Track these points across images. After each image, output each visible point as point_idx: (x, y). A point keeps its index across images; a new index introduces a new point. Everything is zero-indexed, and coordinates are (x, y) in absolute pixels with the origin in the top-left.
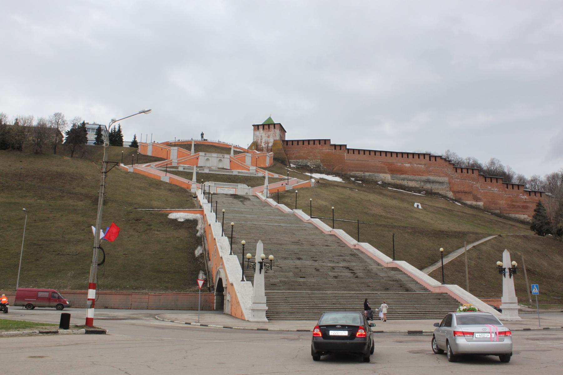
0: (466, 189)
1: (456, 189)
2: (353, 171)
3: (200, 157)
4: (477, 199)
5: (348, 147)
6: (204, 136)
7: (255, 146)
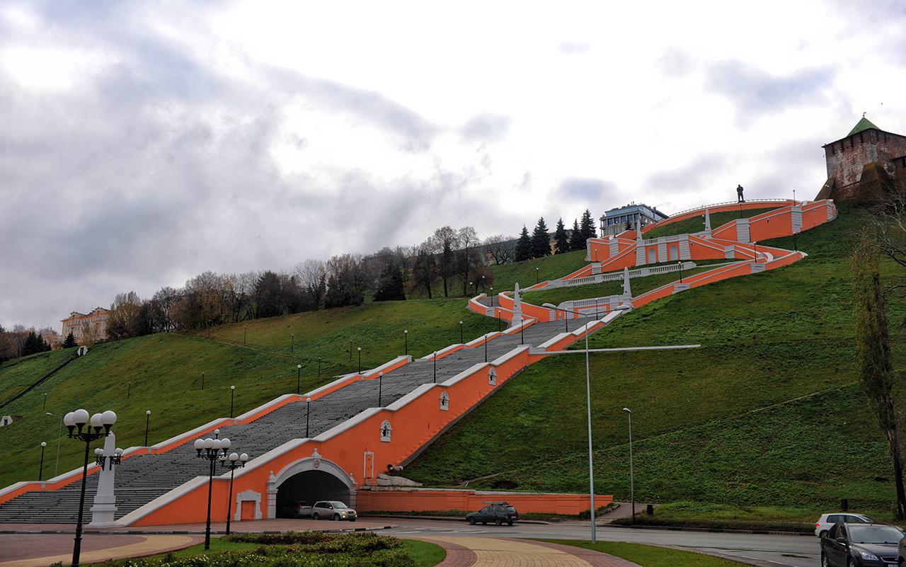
7: (832, 190)
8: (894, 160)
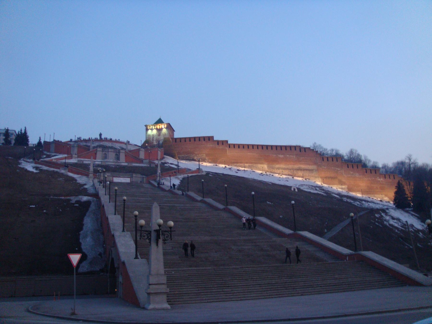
3: (98, 153)
5: (229, 143)
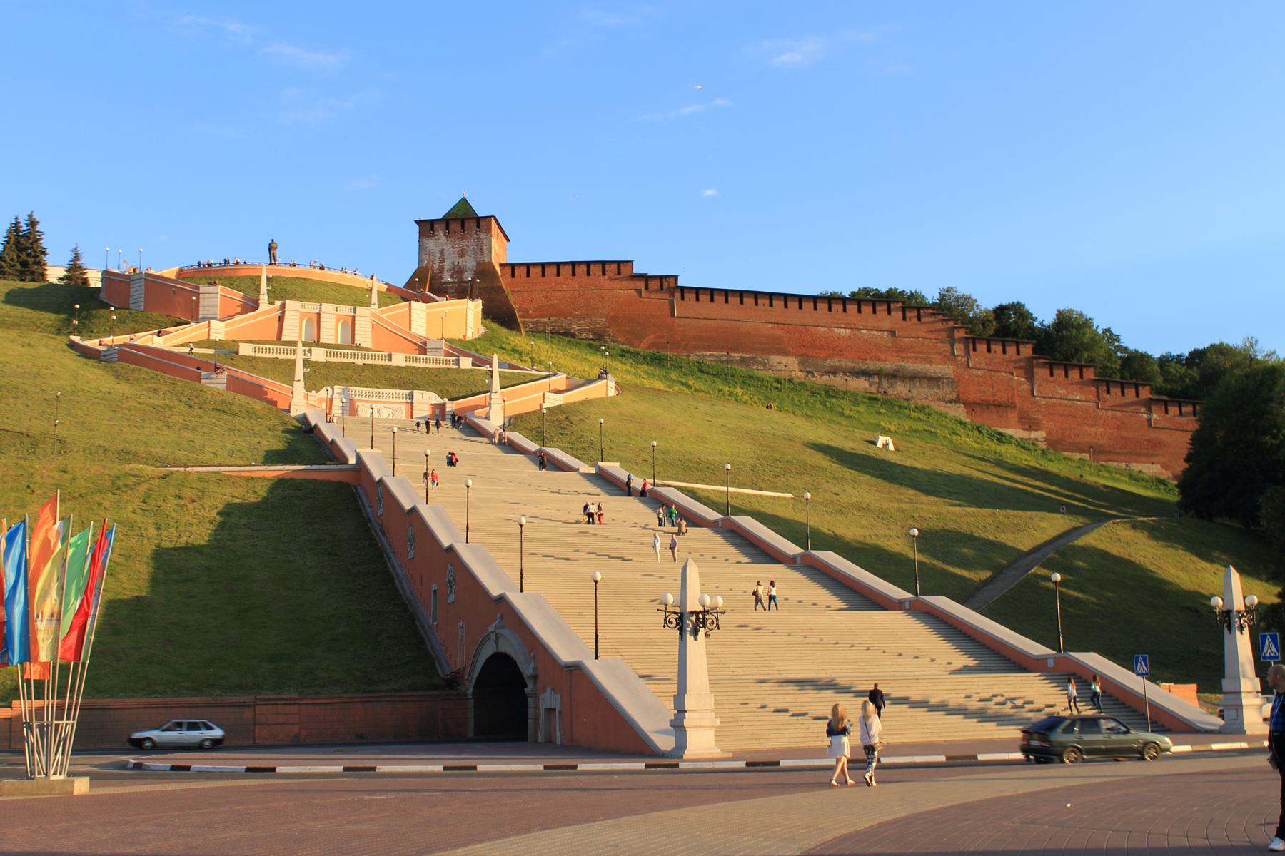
0: (1001, 397)
1: (973, 395)
2: (695, 348)
4: (1028, 423)
6: (278, 253)
8: (502, 265)
